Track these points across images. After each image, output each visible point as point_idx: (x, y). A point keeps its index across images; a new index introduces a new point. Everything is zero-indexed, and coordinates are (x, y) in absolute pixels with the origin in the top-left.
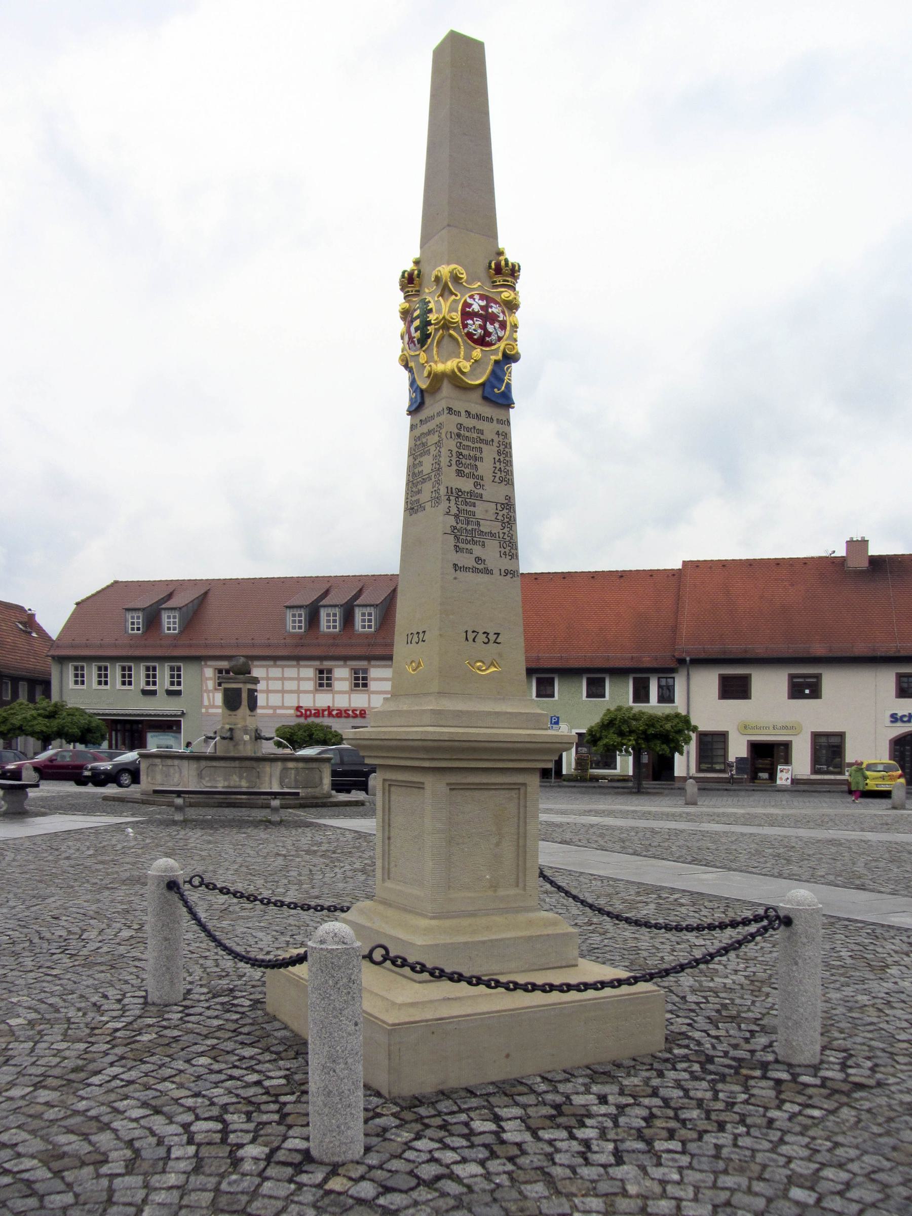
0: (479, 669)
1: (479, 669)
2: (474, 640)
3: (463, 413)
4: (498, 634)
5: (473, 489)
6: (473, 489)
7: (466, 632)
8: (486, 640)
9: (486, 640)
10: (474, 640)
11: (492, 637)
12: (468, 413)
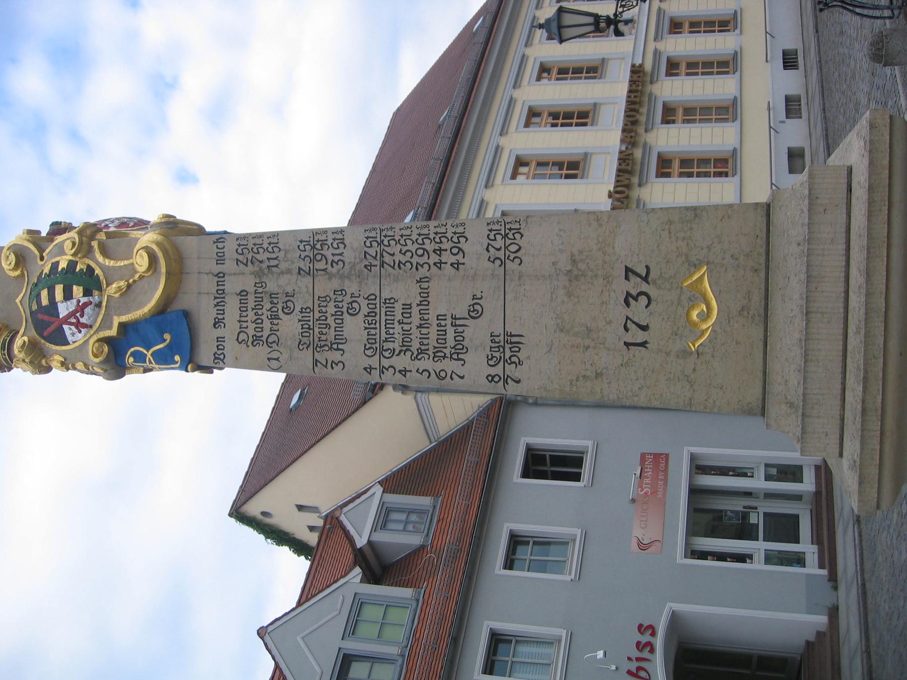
0: (705, 317)
1: (705, 317)
2: (644, 328)
3: (219, 332)
4: (628, 270)
5: (361, 316)
6: (361, 316)
7: (626, 344)
8: (643, 300)
9: (643, 300)
10: (644, 328)
11: (635, 285)
12: (217, 323)
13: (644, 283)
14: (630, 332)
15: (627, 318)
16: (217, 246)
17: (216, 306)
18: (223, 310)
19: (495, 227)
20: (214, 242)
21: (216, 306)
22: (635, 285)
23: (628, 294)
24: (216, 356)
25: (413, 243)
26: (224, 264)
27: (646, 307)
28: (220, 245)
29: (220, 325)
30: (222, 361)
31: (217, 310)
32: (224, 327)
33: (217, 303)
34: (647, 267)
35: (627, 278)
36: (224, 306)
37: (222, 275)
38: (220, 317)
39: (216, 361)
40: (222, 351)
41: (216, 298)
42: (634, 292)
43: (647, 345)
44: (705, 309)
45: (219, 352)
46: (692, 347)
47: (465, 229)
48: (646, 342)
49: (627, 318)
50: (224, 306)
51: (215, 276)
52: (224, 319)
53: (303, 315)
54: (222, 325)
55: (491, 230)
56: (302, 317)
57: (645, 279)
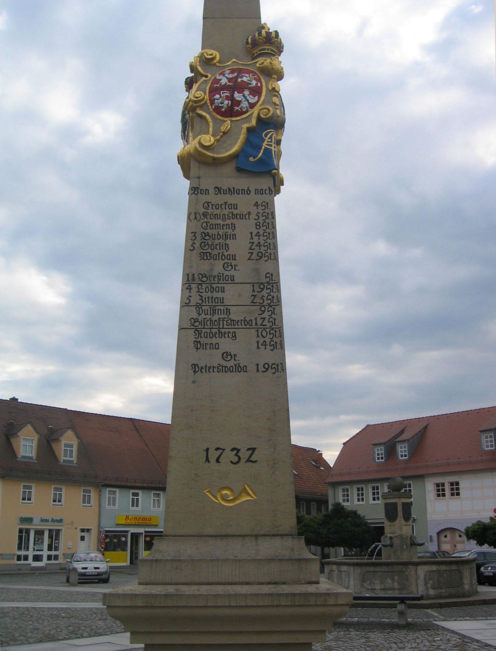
0: (224, 498)
1: (224, 498)
2: (218, 461)
3: (212, 191)
4: (253, 450)
7: (207, 450)
9: (236, 459)
10: (218, 461)
11: (244, 454)
12: (218, 190)
13: (246, 460)
14: (215, 451)
15: (224, 450)
16: (267, 189)
17: (229, 188)
18: (226, 193)
19: (279, 367)
20: (269, 188)
21: (229, 188)
22: (244, 454)
23: (238, 450)
24: (197, 189)
25: (269, 316)
26: (256, 194)
27: (231, 462)
28: (267, 192)
29: (216, 191)
30: (194, 193)
31: (226, 190)
32: (215, 194)
33: (231, 190)
34: (256, 461)
35: (249, 449)
36: (229, 194)
37: (249, 193)
38: (222, 191)
39: (193, 189)
40: (200, 193)
41: (234, 188)
42: (240, 454)
43: (207, 462)
44: (231, 498)
45: (199, 191)
46: (207, 490)
47: (279, 349)
48: (209, 462)
49: (224, 450)
50: (229, 194)
51: (248, 188)
52: (221, 194)
53: (224, 246)
54: (216, 193)
55: (278, 365)
56: (222, 245)
57: (249, 460)
